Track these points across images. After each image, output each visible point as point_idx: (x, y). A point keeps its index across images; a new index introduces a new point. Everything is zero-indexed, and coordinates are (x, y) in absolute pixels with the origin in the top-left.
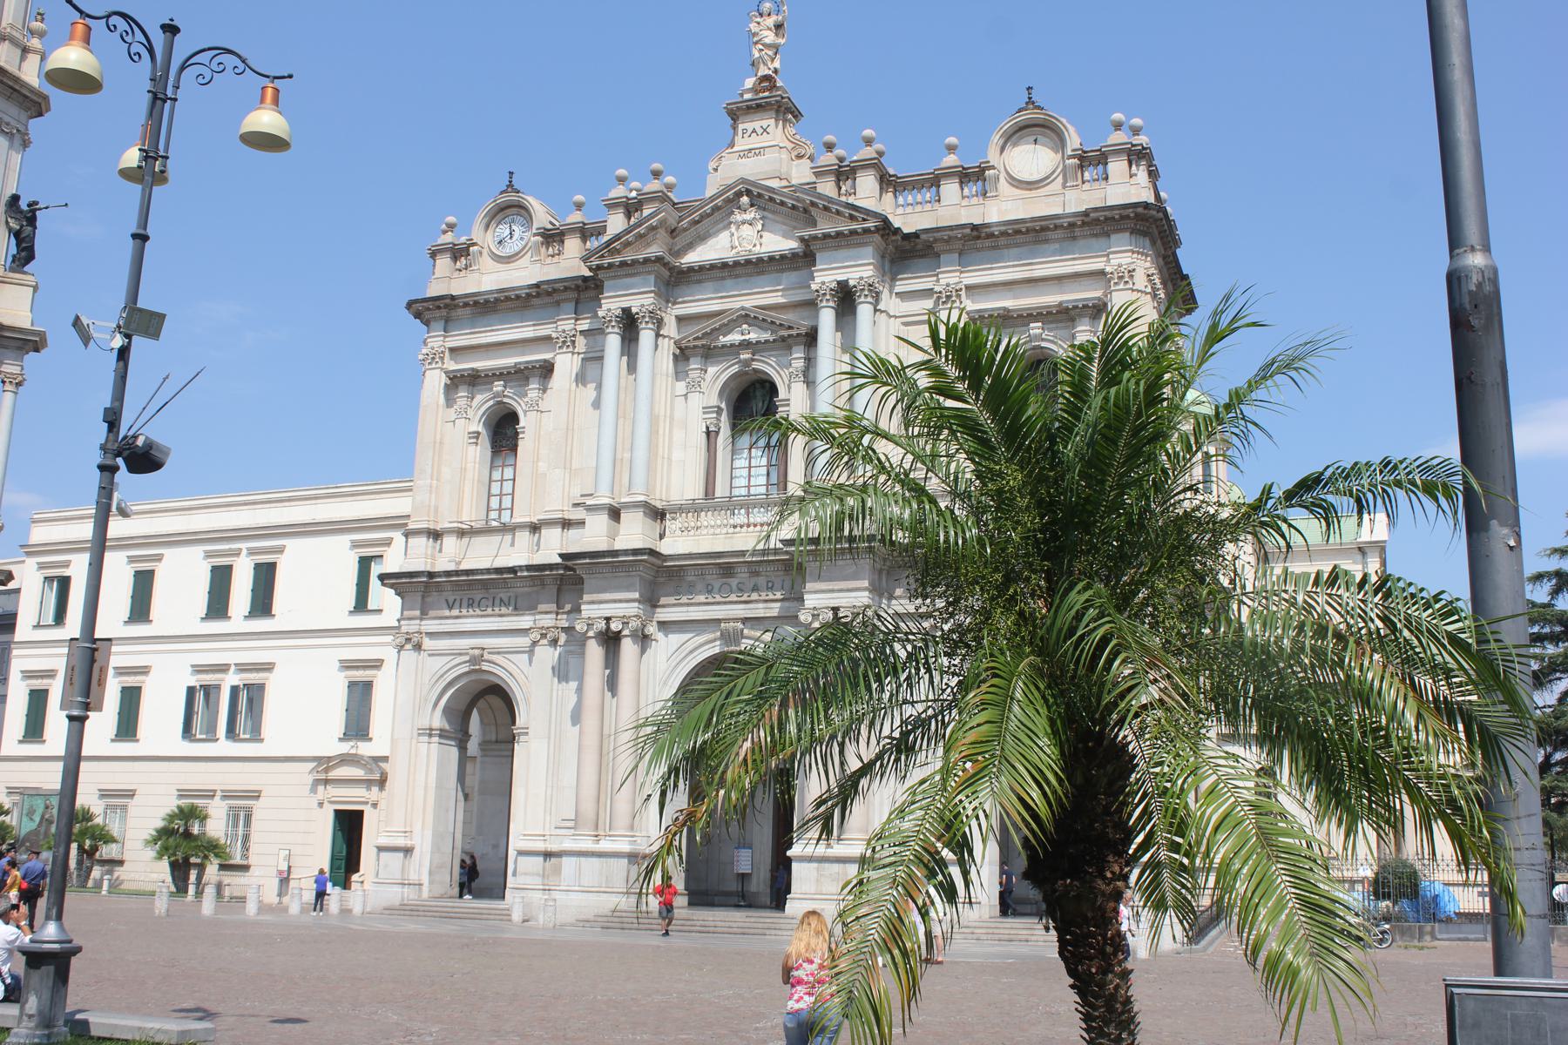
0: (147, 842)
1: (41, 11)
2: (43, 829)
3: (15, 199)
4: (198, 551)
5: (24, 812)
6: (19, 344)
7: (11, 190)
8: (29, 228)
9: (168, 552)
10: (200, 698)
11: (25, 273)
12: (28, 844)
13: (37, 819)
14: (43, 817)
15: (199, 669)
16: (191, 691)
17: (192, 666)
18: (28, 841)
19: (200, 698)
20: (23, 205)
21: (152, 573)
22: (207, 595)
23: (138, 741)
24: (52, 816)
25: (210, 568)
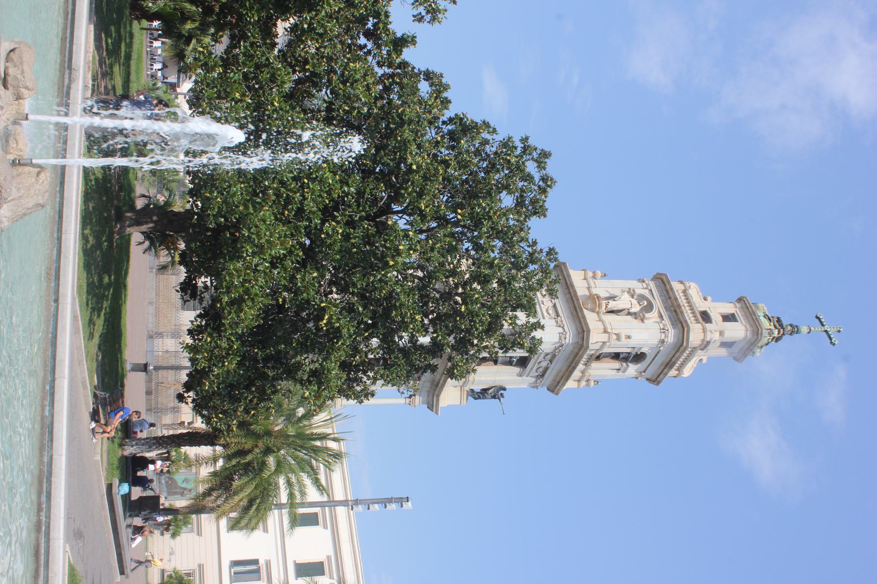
0: (175, 569)
1: (599, 383)
2: (178, 490)
3: (504, 389)
4: (331, 553)
5: (187, 476)
6: (431, 403)
7: (507, 387)
8: (490, 397)
9: (328, 532)
10: (254, 567)
11: (467, 399)
12: (170, 482)
13: (184, 485)
14: (185, 489)
15: (268, 564)
16: (255, 562)
17: (270, 560)
18: (172, 482)
19: (254, 567)
20: (502, 392)
21: (317, 524)
22: (307, 562)
23: (228, 532)
24: (186, 495)
25: (322, 561)
